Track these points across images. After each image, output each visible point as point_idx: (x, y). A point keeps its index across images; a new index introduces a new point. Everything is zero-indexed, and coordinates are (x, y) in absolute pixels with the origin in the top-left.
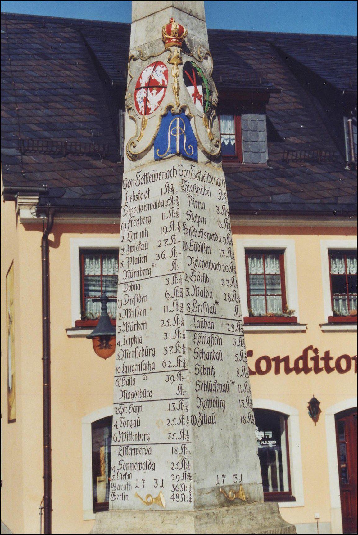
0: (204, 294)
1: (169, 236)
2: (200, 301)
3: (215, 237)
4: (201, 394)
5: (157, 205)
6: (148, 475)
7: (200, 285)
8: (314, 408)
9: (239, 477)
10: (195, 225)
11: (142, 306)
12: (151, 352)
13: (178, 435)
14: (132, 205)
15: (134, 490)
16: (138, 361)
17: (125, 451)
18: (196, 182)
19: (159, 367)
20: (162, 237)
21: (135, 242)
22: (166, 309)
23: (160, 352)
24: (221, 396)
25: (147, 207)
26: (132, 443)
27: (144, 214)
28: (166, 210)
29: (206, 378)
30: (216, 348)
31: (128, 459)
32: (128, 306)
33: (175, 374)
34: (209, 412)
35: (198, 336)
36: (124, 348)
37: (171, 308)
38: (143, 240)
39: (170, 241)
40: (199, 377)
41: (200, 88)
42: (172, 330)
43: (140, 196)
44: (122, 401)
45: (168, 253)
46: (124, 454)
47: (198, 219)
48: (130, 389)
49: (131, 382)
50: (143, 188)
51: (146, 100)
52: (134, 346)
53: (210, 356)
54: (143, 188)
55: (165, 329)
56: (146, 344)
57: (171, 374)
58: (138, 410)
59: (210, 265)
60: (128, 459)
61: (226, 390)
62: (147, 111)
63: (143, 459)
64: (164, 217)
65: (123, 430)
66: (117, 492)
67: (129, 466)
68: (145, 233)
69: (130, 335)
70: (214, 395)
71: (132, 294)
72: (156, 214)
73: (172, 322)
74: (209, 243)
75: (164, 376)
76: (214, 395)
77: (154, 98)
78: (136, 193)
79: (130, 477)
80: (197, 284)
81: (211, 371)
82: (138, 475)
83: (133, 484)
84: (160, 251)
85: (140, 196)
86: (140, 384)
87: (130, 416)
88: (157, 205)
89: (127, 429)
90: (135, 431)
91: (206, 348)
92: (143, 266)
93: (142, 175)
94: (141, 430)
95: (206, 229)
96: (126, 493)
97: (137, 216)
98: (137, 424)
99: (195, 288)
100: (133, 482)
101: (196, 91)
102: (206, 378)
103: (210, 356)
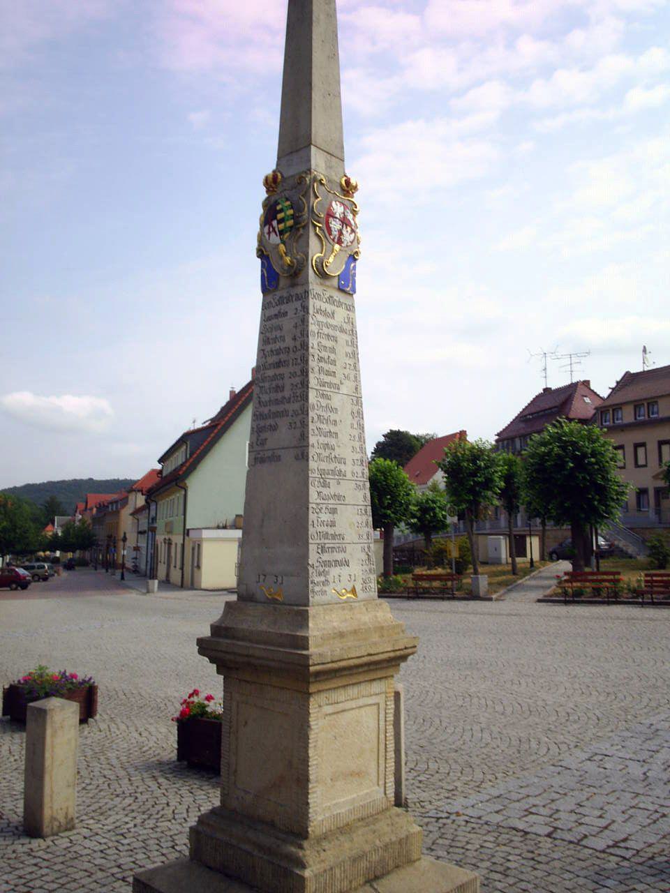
6: (345, 571)
12: (342, 461)
13: (365, 537)
15: (332, 585)
16: (332, 466)
17: (323, 549)
19: (349, 476)
21: (324, 354)
26: (329, 543)
27: (331, 332)
31: (326, 557)
33: (361, 484)
36: (318, 451)
38: (332, 356)
44: (318, 501)
46: (322, 551)
48: (325, 491)
49: (326, 485)
51: (340, 233)
52: (328, 452)
56: (337, 452)
57: (358, 483)
58: (334, 511)
60: (326, 557)
63: (339, 556)
65: (320, 529)
66: (317, 589)
67: (328, 564)
68: (333, 350)
69: (322, 440)
71: (324, 402)
75: (353, 485)
79: (328, 573)
82: (334, 571)
83: (331, 580)
86: (333, 489)
87: (325, 517)
89: (325, 529)
90: (331, 531)
96: (325, 588)
97: (326, 331)
98: (333, 524)
100: (330, 578)
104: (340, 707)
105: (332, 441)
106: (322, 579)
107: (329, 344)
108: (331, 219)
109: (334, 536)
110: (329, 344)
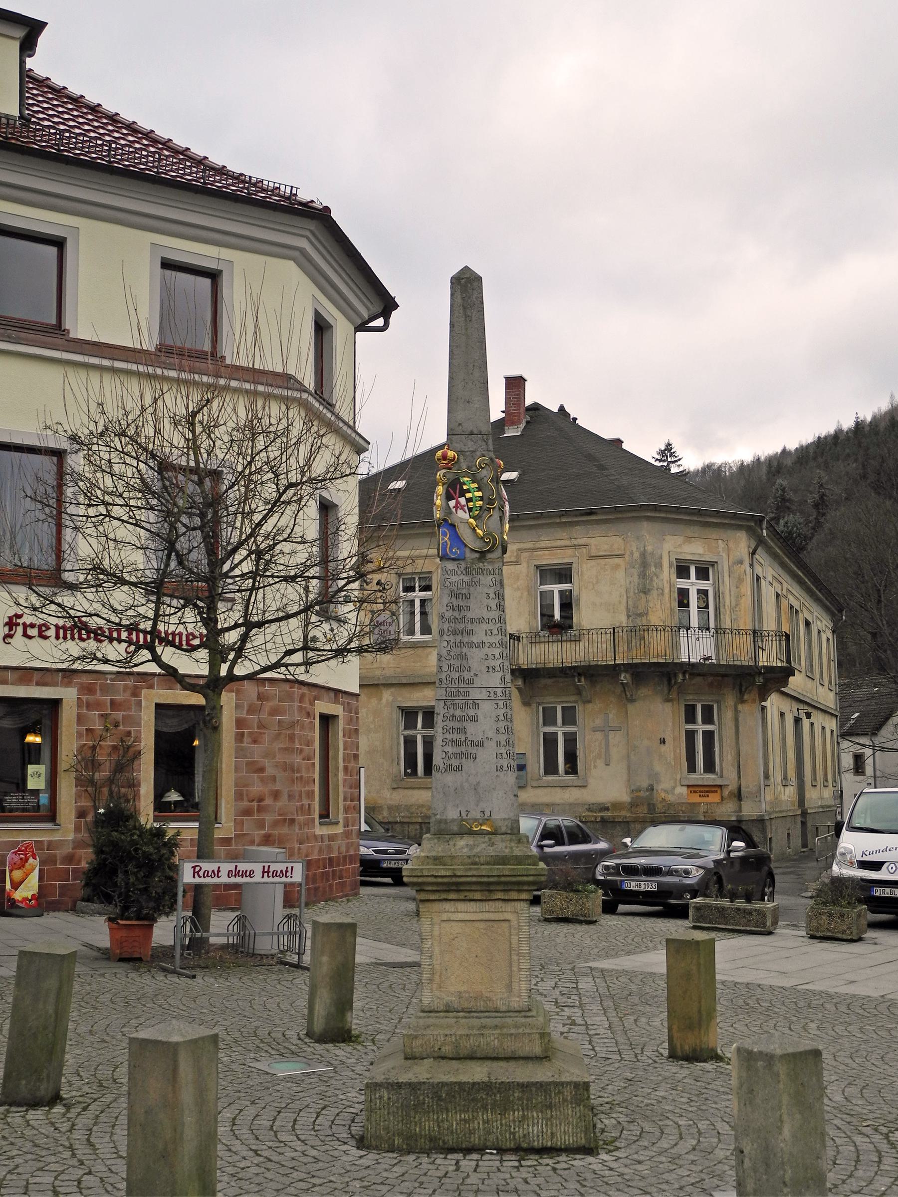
0: (460, 669)
2: (455, 675)
3: (481, 620)
4: (449, 749)
7: (457, 663)
9: (487, 814)
10: (456, 614)
18: (462, 577)
24: (473, 750)
29: (455, 736)
30: (471, 712)
34: (455, 762)
35: (448, 703)
40: (447, 736)
41: (462, 500)
47: (460, 609)
53: (462, 719)
59: (471, 645)
61: (481, 744)
70: (463, 749)
74: (470, 627)
76: (463, 749)
80: (452, 662)
81: (463, 730)
91: (458, 713)
95: (470, 615)
99: (450, 666)
101: (458, 502)
102: (455, 736)
103: (462, 719)
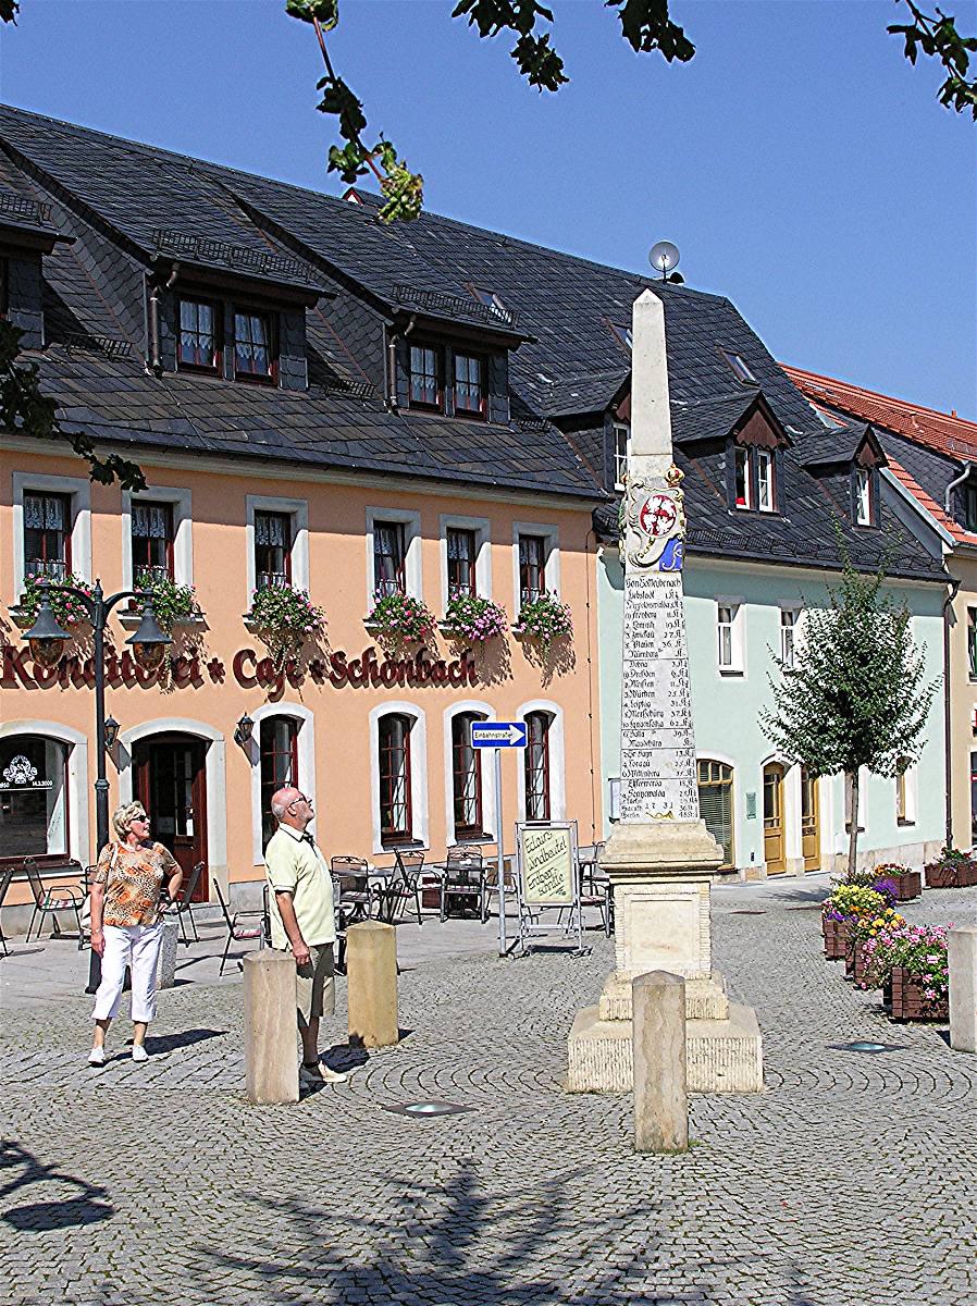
1: (674, 630)
5: (662, 605)
6: (659, 801)
8: (106, 732)
11: (649, 680)
14: (636, 601)
20: (668, 630)
22: (673, 684)
23: (668, 715)
25: (652, 605)
27: (649, 610)
28: (672, 611)
32: (635, 678)
36: (632, 709)
37: (677, 683)
38: (649, 630)
39: (675, 634)
42: (678, 699)
43: (644, 595)
45: (674, 643)
48: (639, 739)
50: (648, 590)
51: (655, 524)
54: (648, 590)
55: (672, 698)
62: (655, 532)
63: (653, 789)
64: (669, 615)
72: (662, 612)
73: (678, 693)
77: (663, 525)
78: (640, 592)
84: (666, 640)
85: (644, 595)
86: (648, 736)
88: (662, 605)
92: (650, 650)
93: (646, 579)
94: (651, 769)
97: (643, 610)
104: (647, 898)
105: (646, 700)
106: (635, 805)
107: (647, 620)
108: (646, 517)
109: (647, 774)
110: (647, 620)
